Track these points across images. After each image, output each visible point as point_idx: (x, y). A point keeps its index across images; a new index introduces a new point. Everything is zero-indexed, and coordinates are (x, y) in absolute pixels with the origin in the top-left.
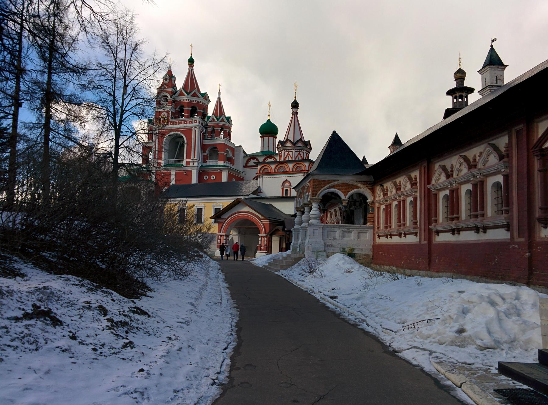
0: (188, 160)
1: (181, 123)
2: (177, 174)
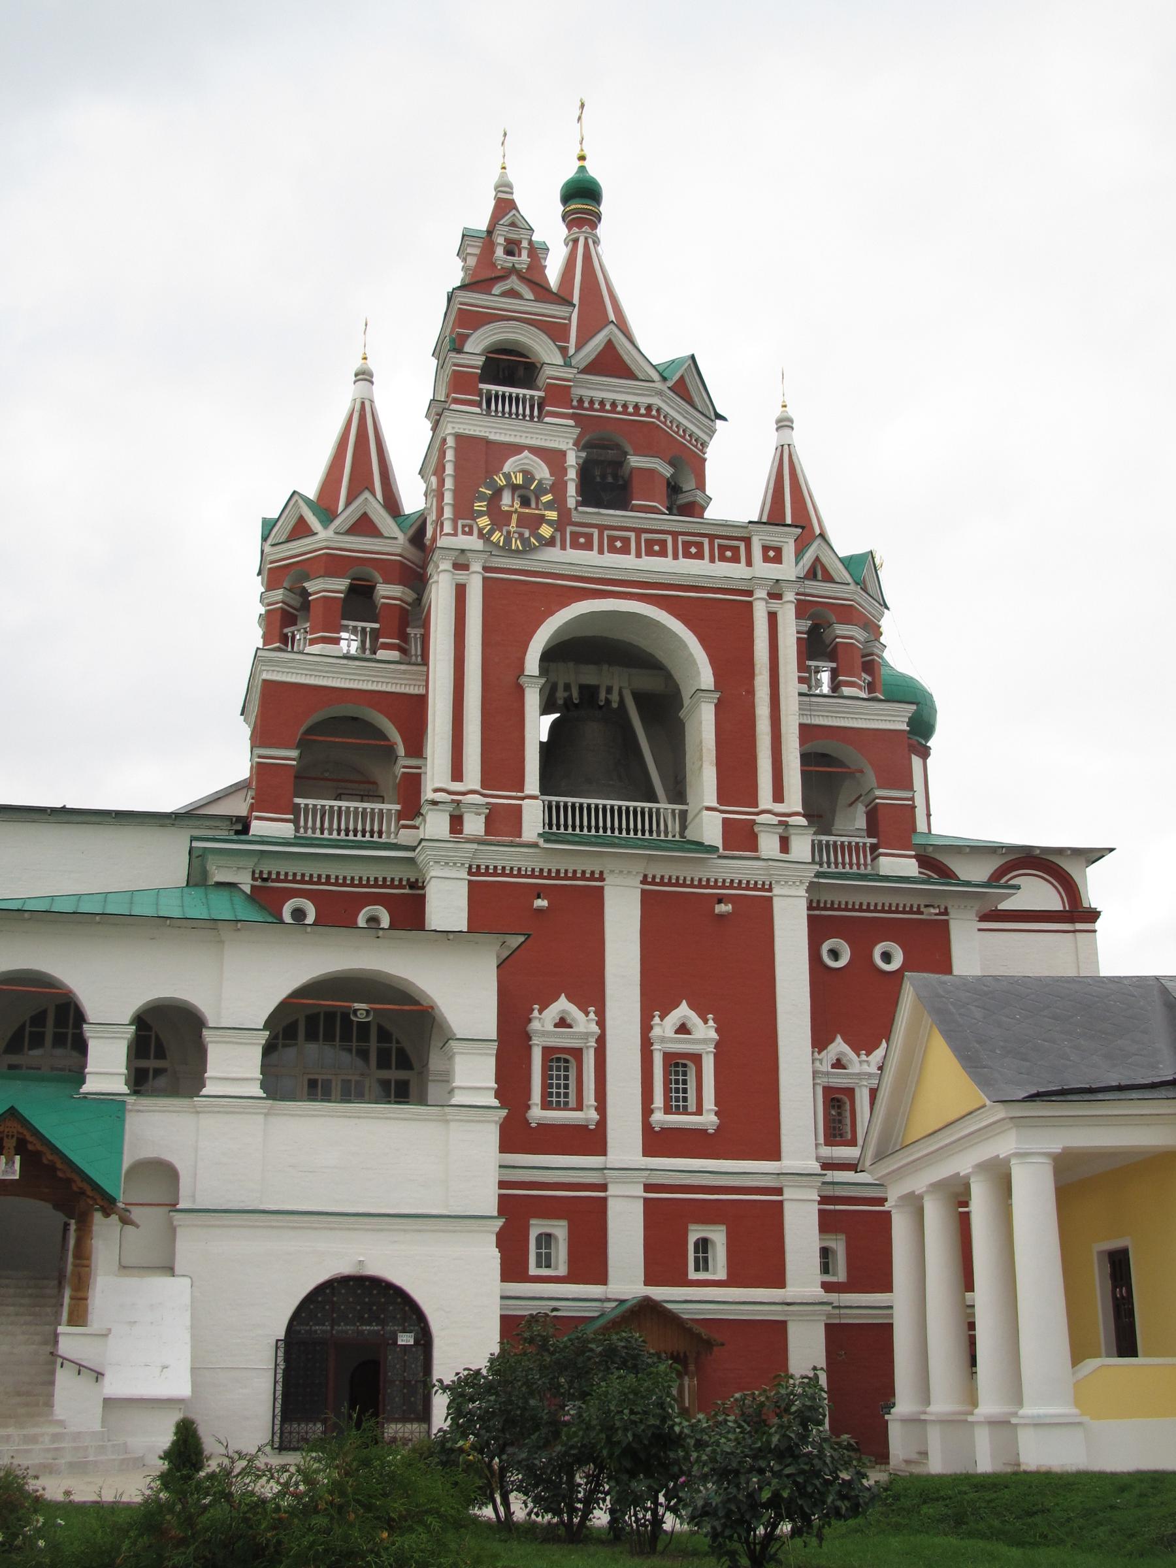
0: (739, 814)
1: (655, 548)
2: (656, 906)
